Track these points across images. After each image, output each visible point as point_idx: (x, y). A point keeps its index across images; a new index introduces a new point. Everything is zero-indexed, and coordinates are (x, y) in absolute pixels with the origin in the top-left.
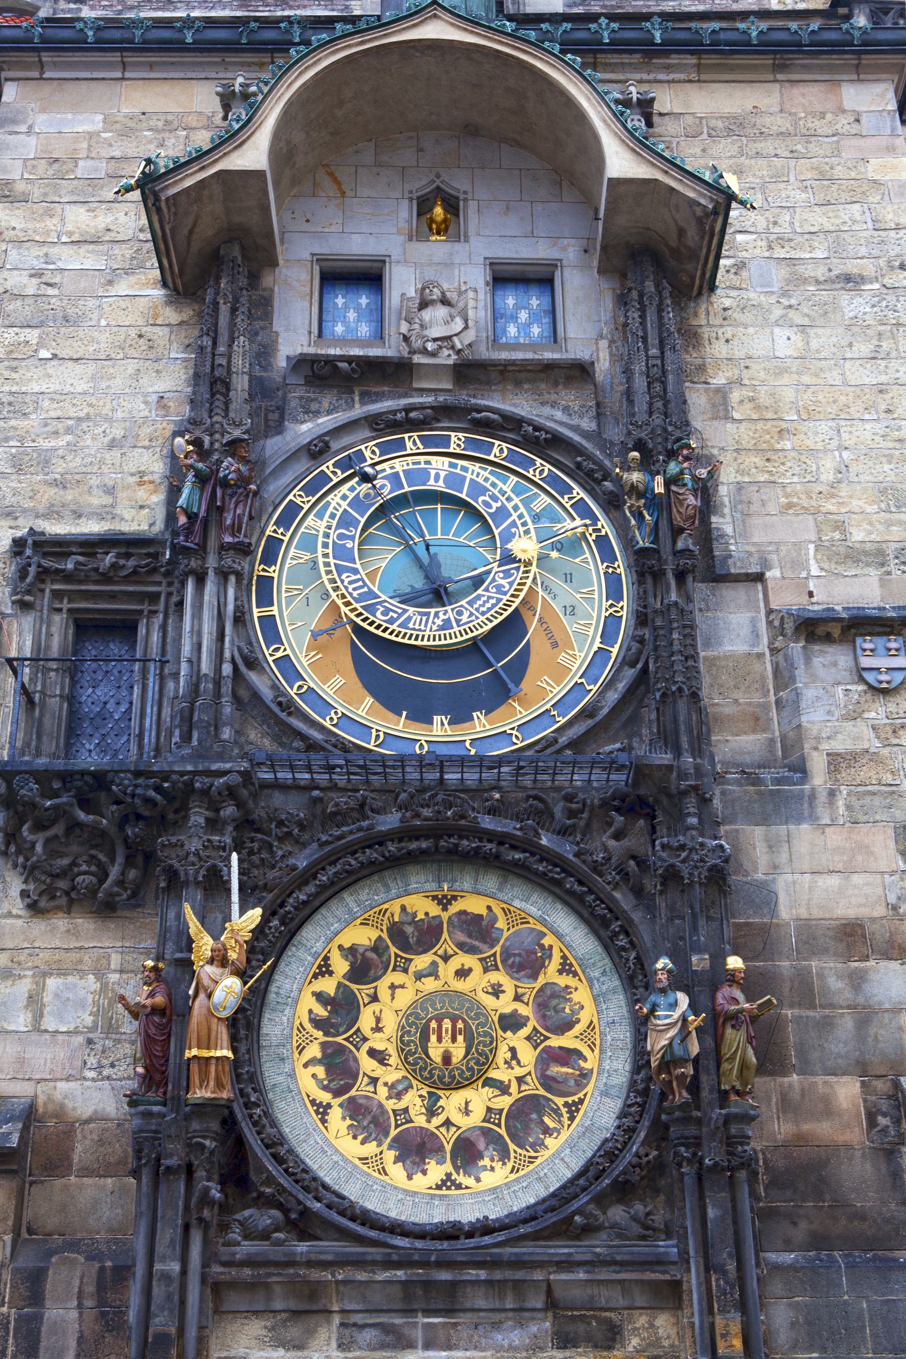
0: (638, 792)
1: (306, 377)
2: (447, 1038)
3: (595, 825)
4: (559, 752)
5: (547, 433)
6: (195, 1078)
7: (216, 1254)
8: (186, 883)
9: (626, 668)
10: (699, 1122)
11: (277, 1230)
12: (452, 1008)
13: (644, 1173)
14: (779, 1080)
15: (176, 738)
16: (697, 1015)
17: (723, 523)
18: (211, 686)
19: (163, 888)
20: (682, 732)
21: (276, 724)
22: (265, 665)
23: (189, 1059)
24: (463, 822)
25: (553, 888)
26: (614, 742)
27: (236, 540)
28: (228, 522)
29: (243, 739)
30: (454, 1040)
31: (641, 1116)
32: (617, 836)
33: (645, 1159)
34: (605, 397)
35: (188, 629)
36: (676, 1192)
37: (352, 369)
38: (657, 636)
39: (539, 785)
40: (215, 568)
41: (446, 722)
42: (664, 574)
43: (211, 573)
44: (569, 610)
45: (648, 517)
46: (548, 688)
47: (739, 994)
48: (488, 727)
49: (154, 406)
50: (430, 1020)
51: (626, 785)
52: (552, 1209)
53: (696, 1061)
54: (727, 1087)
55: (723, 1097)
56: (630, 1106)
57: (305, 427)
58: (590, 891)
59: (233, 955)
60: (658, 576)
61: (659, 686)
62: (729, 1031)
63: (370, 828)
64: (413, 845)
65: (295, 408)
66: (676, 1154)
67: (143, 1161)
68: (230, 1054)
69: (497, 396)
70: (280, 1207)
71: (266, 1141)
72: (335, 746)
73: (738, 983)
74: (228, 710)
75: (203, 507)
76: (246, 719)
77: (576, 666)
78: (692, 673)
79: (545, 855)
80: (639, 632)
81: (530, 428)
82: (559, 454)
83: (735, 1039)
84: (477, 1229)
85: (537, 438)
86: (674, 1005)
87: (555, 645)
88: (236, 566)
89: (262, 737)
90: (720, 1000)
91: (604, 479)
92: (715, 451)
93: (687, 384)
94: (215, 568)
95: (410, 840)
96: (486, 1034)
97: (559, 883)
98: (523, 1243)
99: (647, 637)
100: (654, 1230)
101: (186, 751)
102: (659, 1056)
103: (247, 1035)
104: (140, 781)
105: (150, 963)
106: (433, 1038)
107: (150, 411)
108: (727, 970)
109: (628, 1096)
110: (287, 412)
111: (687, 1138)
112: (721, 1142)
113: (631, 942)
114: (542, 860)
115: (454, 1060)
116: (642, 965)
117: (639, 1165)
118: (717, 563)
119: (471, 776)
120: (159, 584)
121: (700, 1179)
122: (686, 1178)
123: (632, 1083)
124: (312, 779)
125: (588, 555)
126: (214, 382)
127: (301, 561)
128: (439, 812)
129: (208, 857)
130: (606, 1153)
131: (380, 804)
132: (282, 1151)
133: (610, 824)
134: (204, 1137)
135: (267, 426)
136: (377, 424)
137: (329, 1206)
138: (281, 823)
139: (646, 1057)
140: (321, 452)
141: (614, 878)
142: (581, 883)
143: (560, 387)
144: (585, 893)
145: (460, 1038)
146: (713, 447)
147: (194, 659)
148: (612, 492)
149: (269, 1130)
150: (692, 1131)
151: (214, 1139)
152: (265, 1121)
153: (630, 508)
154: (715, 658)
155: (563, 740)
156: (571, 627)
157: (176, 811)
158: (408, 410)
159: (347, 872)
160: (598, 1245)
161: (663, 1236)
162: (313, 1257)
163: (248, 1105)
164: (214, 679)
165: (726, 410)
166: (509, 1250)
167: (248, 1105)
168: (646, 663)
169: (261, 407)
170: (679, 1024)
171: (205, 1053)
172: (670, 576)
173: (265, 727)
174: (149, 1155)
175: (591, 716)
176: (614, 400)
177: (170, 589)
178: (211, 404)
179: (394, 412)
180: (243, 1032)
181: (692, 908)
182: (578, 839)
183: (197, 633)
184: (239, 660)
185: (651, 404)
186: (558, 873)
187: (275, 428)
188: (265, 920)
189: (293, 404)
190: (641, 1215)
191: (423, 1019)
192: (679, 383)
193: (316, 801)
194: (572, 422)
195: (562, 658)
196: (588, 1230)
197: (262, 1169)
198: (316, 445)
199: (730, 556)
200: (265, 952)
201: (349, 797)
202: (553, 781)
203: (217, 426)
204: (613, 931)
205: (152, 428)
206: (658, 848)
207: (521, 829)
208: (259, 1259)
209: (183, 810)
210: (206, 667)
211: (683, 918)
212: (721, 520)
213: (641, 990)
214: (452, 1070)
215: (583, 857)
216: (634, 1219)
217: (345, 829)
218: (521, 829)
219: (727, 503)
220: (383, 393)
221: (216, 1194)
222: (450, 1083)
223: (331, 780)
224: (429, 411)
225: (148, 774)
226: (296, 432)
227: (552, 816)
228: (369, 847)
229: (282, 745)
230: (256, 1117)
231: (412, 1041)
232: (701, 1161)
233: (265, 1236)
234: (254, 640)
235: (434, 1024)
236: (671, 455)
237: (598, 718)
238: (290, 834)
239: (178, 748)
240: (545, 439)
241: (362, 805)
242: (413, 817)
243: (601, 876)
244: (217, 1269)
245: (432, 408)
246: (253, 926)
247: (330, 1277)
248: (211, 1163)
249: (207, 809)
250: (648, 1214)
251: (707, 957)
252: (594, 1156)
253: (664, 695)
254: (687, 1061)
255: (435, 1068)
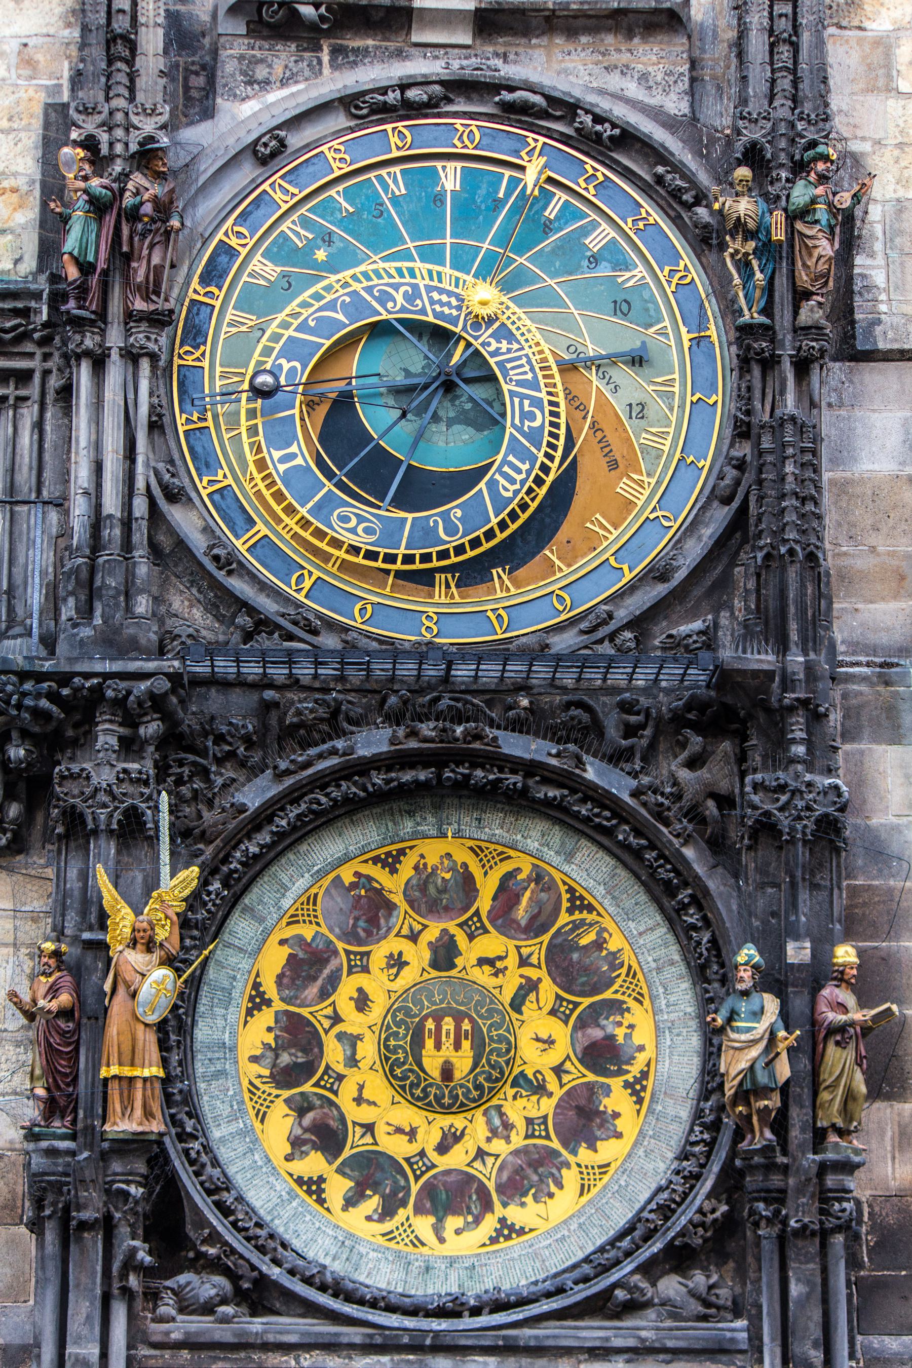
0: (724, 699)
1: (248, 24)
2: (448, 1044)
3: (662, 747)
4: (612, 637)
5: (614, 126)
6: (116, 1104)
7: (144, 1332)
8: (95, 832)
9: (716, 504)
10: (785, 1170)
11: (224, 1302)
12: (456, 1002)
13: (709, 1234)
14: (897, 1106)
15: (68, 610)
16: (787, 1029)
17: (870, 266)
18: (117, 532)
19: (59, 835)
20: (791, 616)
21: (211, 587)
22: (193, 495)
23: (106, 1080)
24: (477, 745)
25: (599, 838)
26: (694, 617)
27: (152, 307)
28: (140, 278)
29: (163, 609)
30: (457, 1046)
31: (708, 1157)
32: (693, 764)
33: (711, 1217)
34: (703, 51)
35: (83, 443)
36: (750, 1259)
37: (321, 17)
38: (763, 465)
39: (584, 684)
40: (121, 349)
41: (453, 585)
42: (779, 362)
43: (115, 355)
44: (636, 410)
45: (759, 275)
46: (601, 532)
47: (847, 997)
48: (513, 591)
49: (14, 60)
50: (425, 1018)
51: (708, 686)
52: (586, 1279)
53: (785, 1089)
54: (825, 1124)
55: (819, 1137)
56: (693, 1144)
57: (249, 108)
58: (652, 846)
59: (161, 934)
60: (769, 364)
61: (762, 543)
62: (831, 1049)
63: (349, 751)
64: (407, 776)
65: (233, 75)
66: (752, 1212)
67: (47, 1212)
68: (162, 1074)
69: (539, 55)
70: (227, 1272)
71: (207, 1185)
72: (295, 623)
73: (848, 982)
74: (143, 570)
75: (103, 255)
76: (167, 577)
77: (643, 499)
78: (811, 520)
79: (590, 793)
80: (737, 453)
81: (588, 119)
82: (631, 158)
83: (838, 1059)
84: (486, 1304)
85: (599, 135)
86: (758, 1014)
87: (613, 465)
88: (152, 346)
89: (191, 606)
90: (822, 1007)
91: (697, 202)
92: (866, 147)
93: (832, 30)
94: (121, 349)
95: (403, 768)
96: (501, 1039)
97: (609, 832)
98: (545, 1324)
99: (749, 458)
100: (718, 1308)
101: (86, 632)
102: (736, 1082)
103: (179, 1042)
104: (28, 686)
105: (49, 946)
106: (430, 1043)
107: (8, 70)
108: (834, 965)
109: (691, 1130)
110: (220, 82)
111: (768, 1191)
112: (812, 1196)
113: (705, 919)
114: (584, 801)
115: (458, 1075)
116: (719, 950)
117: (702, 1225)
118: (859, 331)
119: (490, 671)
120: (31, 355)
121: (782, 1241)
122: (764, 1242)
123: (698, 1114)
124: (265, 674)
125: (667, 323)
126: (112, 39)
127: (244, 329)
128: (444, 730)
129: (124, 794)
130: (660, 1207)
131: (360, 711)
132: (228, 1198)
133: (683, 745)
134: (128, 1182)
135: (188, 98)
136: (357, 107)
137: (292, 1272)
138: (220, 739)
139: (718, 1079)
140: (274, 155)
141: (685, 829)
142: (638, 833)
143: (636, 40)
144: (643, 848)
145: (466, 1044)
146: (863, 139)
147: (92, 491)
148: (706, 226)
149: (209, 1169)
150: (776, 1181)
151: (139, 1184)
152: (204, 1160)
153: (732, 256)
154: (848, 482)
155: (622, 614)
156: (638, 437)
157: (76, 726)
158: (403, 87)
159: (313, 812)
160: (645, 1327)
161: (729, 1316)
162: (271, 1338)
163: (183, 1137)
164: (121, 520)
165: (889, 77)
166: (527, 1332)
167: (183, 1137)
168: (746, 500)
169: (178, 66)
170: (764, 1042)
171: (127, 1072)
172: (787, 368)
173: (194, 591)
174: (54, 1204)
175: (663, 577)
176: (717, 54)
177: (49, 364)
178: (108, 78)
179: (384, 91)
180: (173, 1037)
181: (792, 877)
182: (637, 768)
183: (97, 446)
184: (157, 492)
185: (773, 81)
186: (608, 820)
187: (200, 101)
188: (204, 882)
189: (229, 67)
190: (703, 1289)
191: (415, 1016)
192: (820, 44)
193: (268, 706)
194: (653, 102)
195: (624, 487)
196: (633, 1307)
197: (202, 1222)
198: (265, 145)
199: (879, 322)
200: (202, 924)
201: (316, 701)
202: (605, 680)
203: (119, 116)
204: (681, 902)
205: (12, 98)
206: (748, 789)
207: (558, 755)
208: (202, 1340)
209: (87, 723)
210: (111, 505)
211: (777, 886)
212: (869, 262)
213: (716, 985)
214: (455, 1088)
215: (643, 797)
216: (692, 1293)
217: (313, 751)
218: (558, 755)
219: (880, 234)
220: (366, 51)
221: (144, 1256)
222: (451, 1106)
223: (291, 675)
224: (437, 88)
225: (40, 677)
226: (233, 117)
227: (601, 734)
228: (348, 778)
229: (218, 618)
230: (193, 1154)
231: (401, 1047)
232: (785, 1222)
233: (208, 1309)
234: (176, 456)
235: (430, 1024)
236: (799, 168)
237: (674, 583)
238: (232, 755)
239: (75, 626)
240: (611, 138)
241: (335, 713)
242: (407, 736)
243: (667, 824)
244: (144, 1351)
245: (441, 83)
246: (187, 892)
247: (293, 1363)
248: (136, 1214)
249: (121, 725)
250: (711, 1287)
251: (808, 944)
252: (642, 1209)
253: (768, 557)
254: (772, 1090)
255: (431, 1085)
